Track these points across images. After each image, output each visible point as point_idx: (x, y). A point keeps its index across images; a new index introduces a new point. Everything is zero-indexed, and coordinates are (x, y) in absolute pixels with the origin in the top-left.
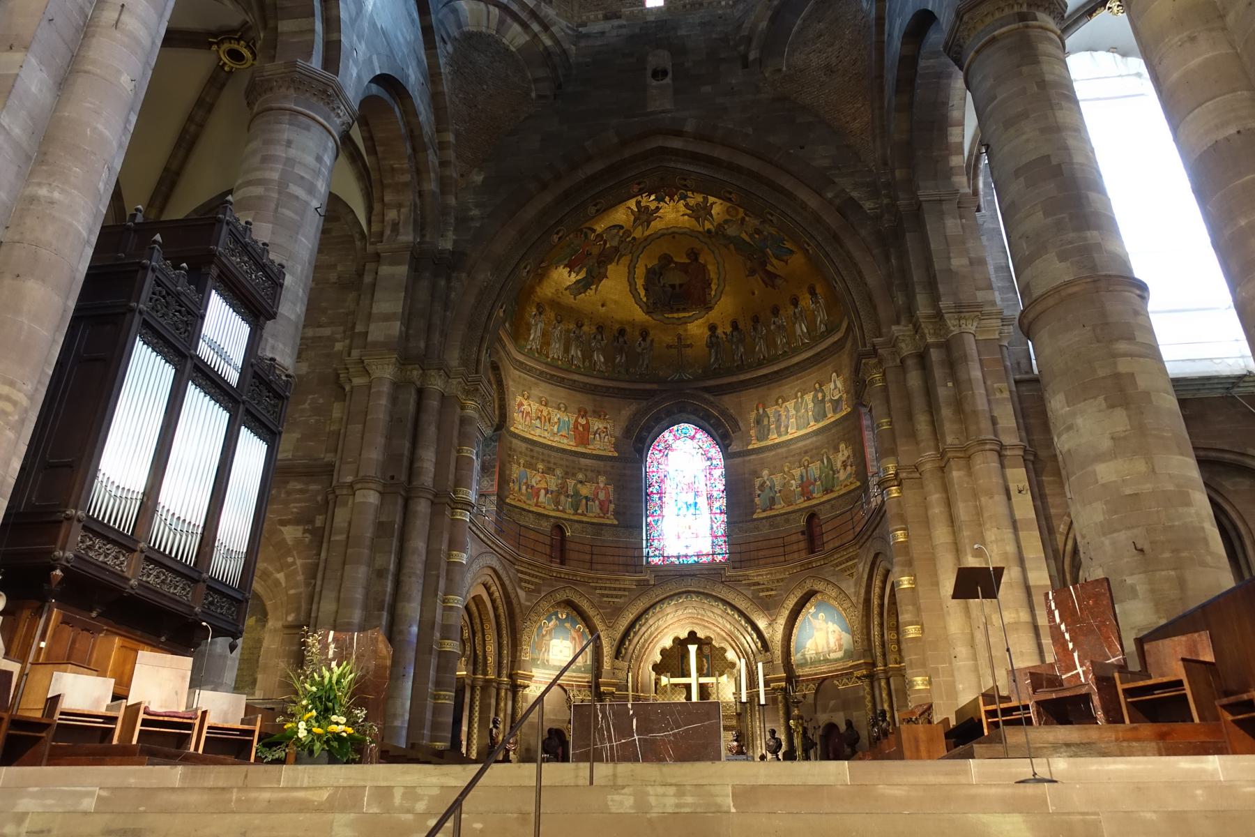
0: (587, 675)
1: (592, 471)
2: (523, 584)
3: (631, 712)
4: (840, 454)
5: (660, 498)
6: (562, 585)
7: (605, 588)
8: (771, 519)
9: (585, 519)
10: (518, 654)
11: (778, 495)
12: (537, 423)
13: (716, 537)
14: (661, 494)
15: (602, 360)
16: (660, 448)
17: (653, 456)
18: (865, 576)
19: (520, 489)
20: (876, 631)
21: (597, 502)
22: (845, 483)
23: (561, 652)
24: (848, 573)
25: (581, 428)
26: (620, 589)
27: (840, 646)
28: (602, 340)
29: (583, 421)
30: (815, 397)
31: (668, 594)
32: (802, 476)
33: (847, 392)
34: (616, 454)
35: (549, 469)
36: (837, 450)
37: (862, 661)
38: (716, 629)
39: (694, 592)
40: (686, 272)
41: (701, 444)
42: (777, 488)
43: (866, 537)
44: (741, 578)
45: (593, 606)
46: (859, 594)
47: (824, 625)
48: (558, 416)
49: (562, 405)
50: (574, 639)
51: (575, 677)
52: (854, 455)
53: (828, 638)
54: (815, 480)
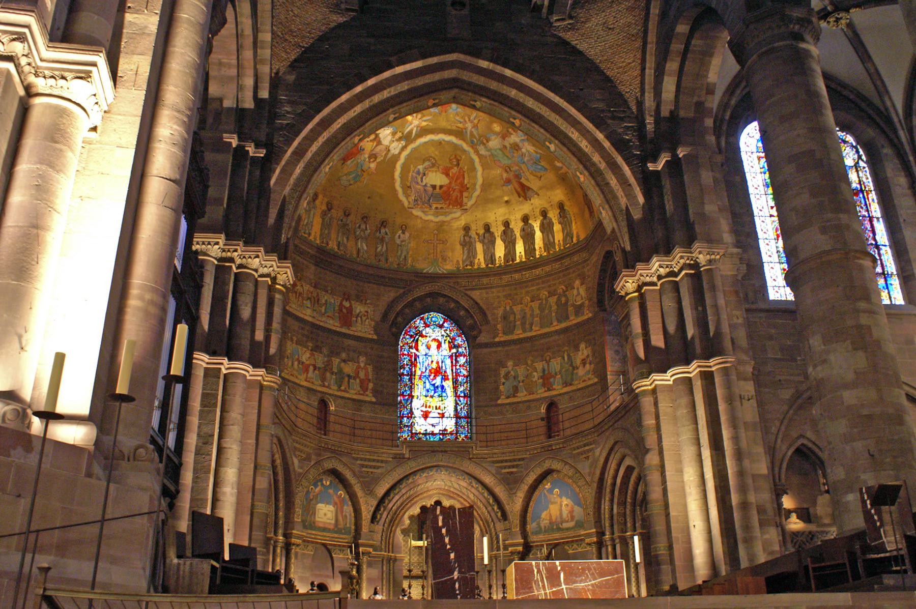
0: (346, 536)
1: (354, 351)
2: (297, 453)
3: (559, 568)
4: (580, 353)
5: (410, 380)
6: (329, 455)
7: (365, 460)
8: (514, 406)
9: (347, 395)
10: (292, 516)
11: (521, 384)
12: (308, 303)
13: (460, 418)
14: (411, 375)
15: (365, 248)
16: (412, 333)
17: (405, 340)
18: (602, 460)
19: (293, 365)
20: (605, 506)
21: (358, 381)
22: (584, 378)
23: (325, 515)
24: (585, 456)
25: (344, 311)
26: (378, 461)
27: (572, 518)
28: (366, 229)
29: (347, 304)
30: (559, 299)
31: (421, 467)
32: (544, 370)
33: (590, 300)
34: (375, 337)
35: (317, 346)
36: (577, 348)
37: (594, 530)
38: (460, 499)
39: (443, 466)
40: (447, 175)
41: (448, 332)
42: (521, 378)
43: (606, 427)
44: (486, 456)
45: (355, 475)
46: (594, 474)
47: (559, 500)
48: (326, 298)
49: (329, 288)
50: (335, 504)
51: (337, 538)
52: (593, 355)
53: (561, 510)
54: (556, 374)
